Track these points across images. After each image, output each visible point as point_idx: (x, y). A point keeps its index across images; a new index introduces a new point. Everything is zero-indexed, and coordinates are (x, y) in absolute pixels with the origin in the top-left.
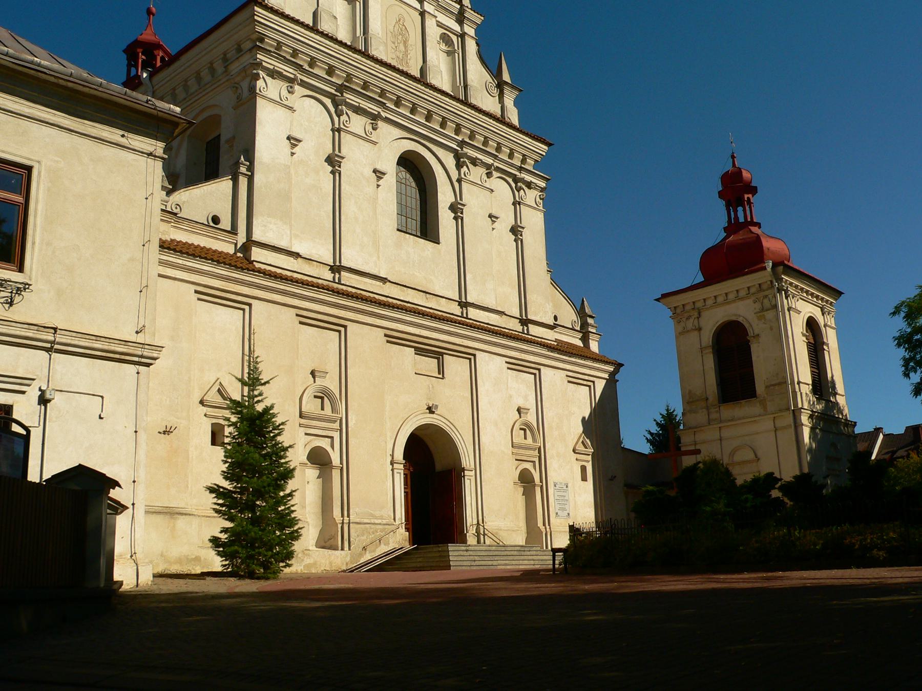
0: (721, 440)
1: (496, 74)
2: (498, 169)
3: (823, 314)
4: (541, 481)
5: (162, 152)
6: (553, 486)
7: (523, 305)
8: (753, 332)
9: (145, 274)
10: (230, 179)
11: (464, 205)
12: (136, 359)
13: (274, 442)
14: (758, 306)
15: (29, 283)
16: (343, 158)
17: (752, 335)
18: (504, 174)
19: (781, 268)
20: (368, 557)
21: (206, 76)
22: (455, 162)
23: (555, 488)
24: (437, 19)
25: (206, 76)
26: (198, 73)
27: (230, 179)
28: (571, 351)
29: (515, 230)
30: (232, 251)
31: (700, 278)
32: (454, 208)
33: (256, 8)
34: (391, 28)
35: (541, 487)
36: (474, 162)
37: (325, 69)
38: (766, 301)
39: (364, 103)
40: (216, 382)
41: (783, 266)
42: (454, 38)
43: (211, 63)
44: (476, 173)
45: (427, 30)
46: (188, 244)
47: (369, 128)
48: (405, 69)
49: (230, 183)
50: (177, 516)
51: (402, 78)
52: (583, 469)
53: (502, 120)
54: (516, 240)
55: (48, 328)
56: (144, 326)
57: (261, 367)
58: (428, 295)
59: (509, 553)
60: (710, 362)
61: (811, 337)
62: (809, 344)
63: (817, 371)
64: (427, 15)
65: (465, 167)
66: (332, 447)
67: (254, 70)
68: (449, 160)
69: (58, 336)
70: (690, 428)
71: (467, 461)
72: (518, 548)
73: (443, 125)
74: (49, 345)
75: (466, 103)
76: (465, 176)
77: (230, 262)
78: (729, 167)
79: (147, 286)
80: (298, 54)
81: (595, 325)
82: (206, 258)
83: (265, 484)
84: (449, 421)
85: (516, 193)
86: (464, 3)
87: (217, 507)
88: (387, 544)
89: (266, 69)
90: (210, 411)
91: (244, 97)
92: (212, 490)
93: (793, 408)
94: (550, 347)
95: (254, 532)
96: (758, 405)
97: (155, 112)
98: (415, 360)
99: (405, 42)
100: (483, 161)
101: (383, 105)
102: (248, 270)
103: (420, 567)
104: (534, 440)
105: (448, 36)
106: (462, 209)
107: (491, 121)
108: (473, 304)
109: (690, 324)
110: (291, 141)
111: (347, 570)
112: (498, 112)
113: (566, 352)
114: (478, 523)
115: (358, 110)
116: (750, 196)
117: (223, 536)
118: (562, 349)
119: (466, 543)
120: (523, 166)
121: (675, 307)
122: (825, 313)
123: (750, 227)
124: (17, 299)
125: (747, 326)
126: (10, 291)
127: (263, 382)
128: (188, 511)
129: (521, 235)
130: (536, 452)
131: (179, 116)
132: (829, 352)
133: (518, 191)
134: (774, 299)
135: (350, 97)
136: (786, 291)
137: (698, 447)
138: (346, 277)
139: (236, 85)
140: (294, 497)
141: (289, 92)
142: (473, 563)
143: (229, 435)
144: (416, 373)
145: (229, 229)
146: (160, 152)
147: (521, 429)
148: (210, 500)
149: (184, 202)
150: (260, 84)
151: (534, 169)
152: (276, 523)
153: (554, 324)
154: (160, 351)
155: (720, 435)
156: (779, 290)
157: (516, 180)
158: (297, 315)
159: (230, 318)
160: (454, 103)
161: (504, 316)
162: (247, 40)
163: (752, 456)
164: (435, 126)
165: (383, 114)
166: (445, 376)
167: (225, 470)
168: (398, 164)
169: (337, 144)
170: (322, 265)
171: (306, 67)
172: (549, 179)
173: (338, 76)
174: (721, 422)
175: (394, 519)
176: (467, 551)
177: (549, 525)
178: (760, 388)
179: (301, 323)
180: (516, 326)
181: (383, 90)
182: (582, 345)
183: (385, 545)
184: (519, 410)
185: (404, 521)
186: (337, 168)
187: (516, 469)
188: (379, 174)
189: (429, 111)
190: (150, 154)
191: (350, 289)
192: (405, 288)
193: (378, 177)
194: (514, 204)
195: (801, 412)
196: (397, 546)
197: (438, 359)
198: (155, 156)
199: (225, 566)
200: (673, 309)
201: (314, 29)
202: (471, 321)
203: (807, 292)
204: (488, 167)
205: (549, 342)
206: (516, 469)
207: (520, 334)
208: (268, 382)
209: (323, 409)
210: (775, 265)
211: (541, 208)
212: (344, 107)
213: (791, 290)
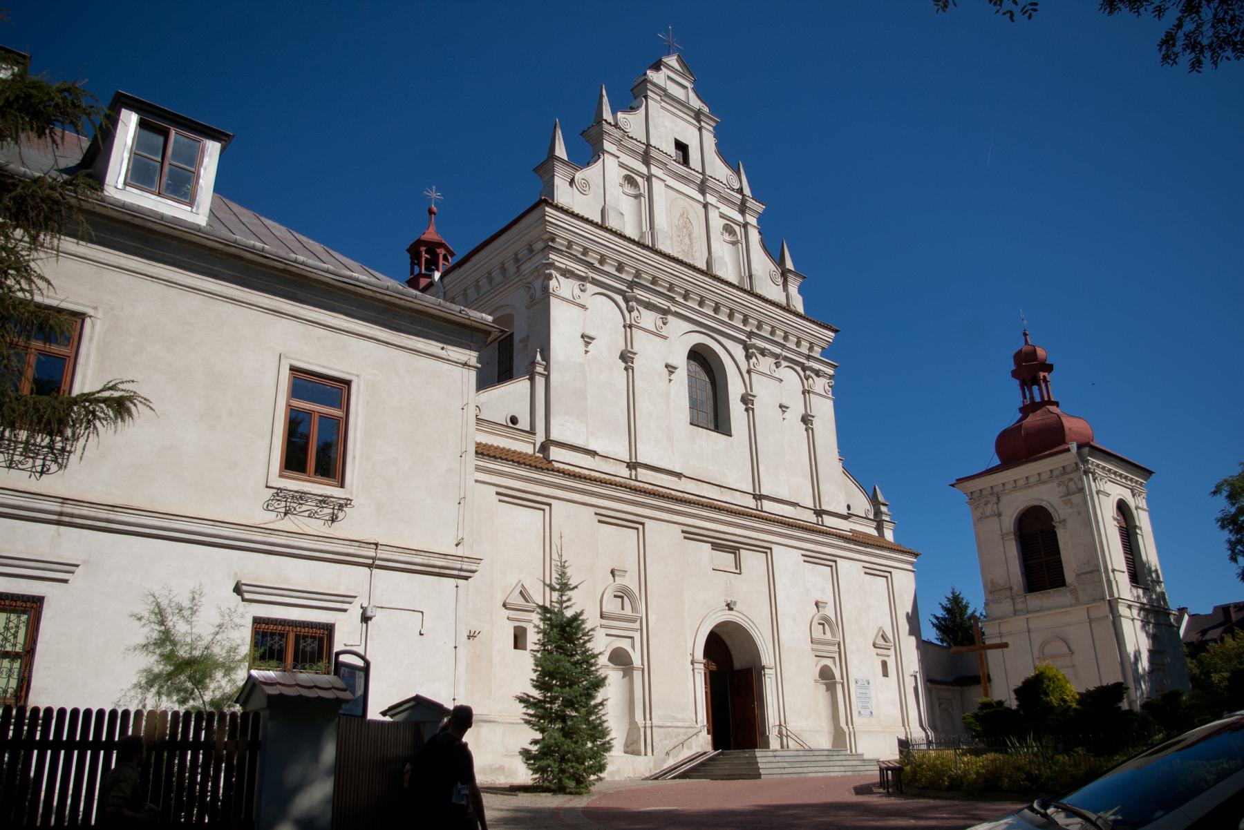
0: (1029, 631)
1: (780, 262)
2: (786, 358)
3: (1134, 495)
4: (842, 678)
5: (475, 361)
6: (854, 683)
7: (817, 496)
8: (1059, 516)
9: (462, 484)
10: (528, 379)
11: (754, 396)
12: (456, 573)
13: (583, 649)
14: (1063, 489)
15: (351, 498)
16: (635, 354)
17: (1058, 520)
18: (794, 364)
19: (1086, 450)
20: (671, 762)
21: (498, 277)
22: (745, 353)
24: (720, 210)
25: (498, 277)
26: (489, 273)
27: (528, 379)
28: (870, 542)
29: (806, 420)
30: (530, 451)
31: (997, 461)
32: (747, 400)
33: (547, 209)
34: (676, 221)
35: (843, 684)
36: (763, 352)
37: (614, 266)
38: (1071, 484)
39: (653, 298)
40: (517, 585)
41: (1088, 448)
42: (737, 228)
43: (503, 264)
44: (765, 364)
45: (711, 222)
46: (488, 445)
47: (659, 323)
48: (691, 262)
49: (528, 383)
50: (482, 724)
51: (691, 272)
52: (884, 664)
53: (787, 309)
54: (806, 430)
55: (370, 544)
56: (462, 539)
57: (569, 572)
58: (722, 488)
59: (818, 759)
60: (1013, 550)
61: (1123, 520)
62: (1121, 528)
63: (1132, 557)
64: (709, 207)
65: (754, 358)
66: (633, 647)
67: (547, 269)
68: (738, 351)
69: (379, 551)
70: (994, 619)
71: (767, 659)
72: (826, 753)
73: (731, 316)
74: (370, 561)
75: (751, 293)
76: (754, 367)
77: (530, 462)
78: (1020, 345)
79: (464, 498)
80: (588, 252)
81: (889, 513)
82: (506, 459)
83: (578, 694)
84: (747, 617)
85: (805, 381)
86: (745, 193)
87: (527, 717)
88: (690, 748)
89: (558, 269)
90: (513, 614)
91: (537, 296)
92: (521, 700)
93: (1108, 598)
94: (846, 538)
95: (568, 745)
96: (1068, 594)
97: (468, 322)
98: (712, 555)
99: (690, 235)
101: (672, 299)
102: (548, 469)
103: (728, 775)
104: (833, 634)
105: (731, 226)
106: (753, 401)
107: (778, 310)
108: (767, 496)
109: (989, 510)
110: (585, 339)
111: (651, 776)
112: (783, 301)
113: (862, 542)
114: (780, 725)
115: (649, 306)
116: (1046, 374)
117: (534, 749)
118: (856, 539)
119: (769, 748)
120: (811, 354)
121: (972, 493)
122: (1135, 494)
123: (1047, 406)
124: (341, 515)
125: (1051, 510)
126: (332, 507)
127: (571, 587)
128: (492, 717)
129: (812, 424)
130: (836, 648)
131: (492, 325)
132: (1142, 536)
133: (807, 379)
134: (1080, 481)
135: (638, 292)
136: (1093, 474)
137: (1004, 640)
138: (643, 474)
139: (529, 285)
140: (605, 707)
141: (582, 291)
142: (783, 771)
143: (538, 642)
144: (713, 569)
145: (528, 428)
146: (473, 361)
147: (820, 624)
148: (520, 709)
149: (483, 403)
150: (553, 284)
151: (821, 356)
152: (588, 735)
153: (848, 513)
154: (479, 564)
155: (1028, 626)
156: (1086, 472)
157: (804, 368)
158: (596, 514)
159: (529, 519)
160: (742, 294)
161: (798, 508)
162: (538, 240)
163: (1066, 649)
164: (722, 316)
165: (673, 309)
166: (742, 571)
167: (535, 678)
168: (688, 358)
169: (628, 340)
170: (618, 462)
171: (597, 265)
172: (837, 366)
173: (628, 273)
174: (1028, 612)
175: (696, 722)
176: (775, 756)
177: (852, 725)
178: (1069, 576)
179: (599, 521)
180: (810, 517)
181: (671, 284)
182: (877, 535)
183: (688, 749)
184: (817, 604)
185: (705, 723)
186: (630, 364)
187: (816, 665)
188: (671, 369)
189: (717, 303)
190: (465, 365)
191: (647, 486)
192: (700, 483)
193: (670, 371)
194: (803, 393)
195: (1118, 602)
196: (701, 750)
197: (735, 553)
198: (469, 366)
199: (536, 779)
200: (970, 494)
201: (602, 227)
202: (766, 514)
203: (1115, 473)
204: (777, 356)
205: (845, 533)
206: (816, 665)
207: (815, 526)
208: (576, 587)
209: (623, 609)
210: (1080, 447)
211: (830, 396)
212: (634, 303)
213: (1098, 471)
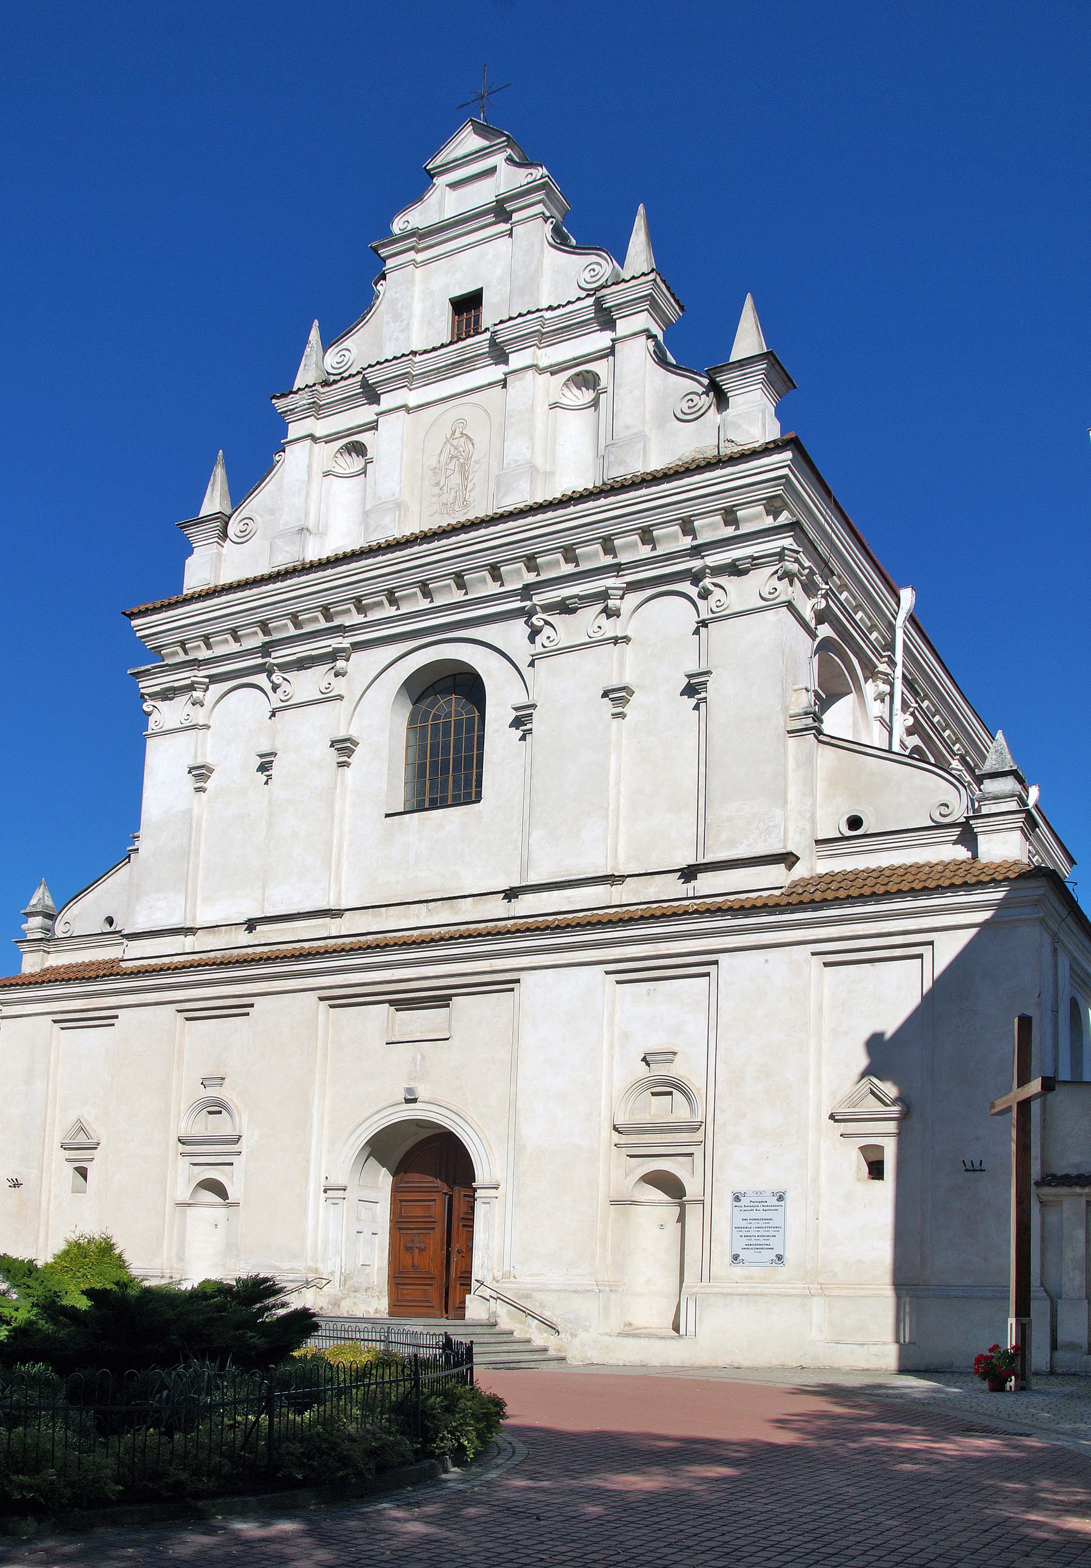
6: (729, 1199)
23: (736, 1204)
36: (565, 608)
100: (581, 594)
164: (478, 592)
